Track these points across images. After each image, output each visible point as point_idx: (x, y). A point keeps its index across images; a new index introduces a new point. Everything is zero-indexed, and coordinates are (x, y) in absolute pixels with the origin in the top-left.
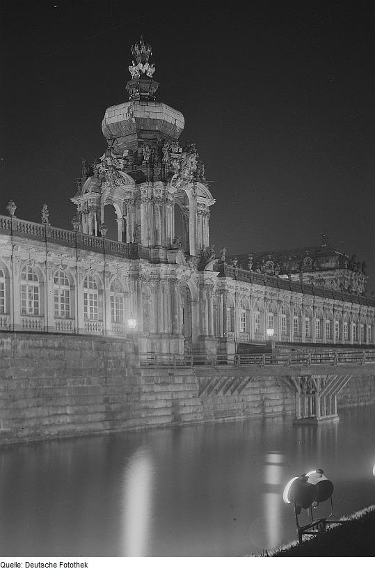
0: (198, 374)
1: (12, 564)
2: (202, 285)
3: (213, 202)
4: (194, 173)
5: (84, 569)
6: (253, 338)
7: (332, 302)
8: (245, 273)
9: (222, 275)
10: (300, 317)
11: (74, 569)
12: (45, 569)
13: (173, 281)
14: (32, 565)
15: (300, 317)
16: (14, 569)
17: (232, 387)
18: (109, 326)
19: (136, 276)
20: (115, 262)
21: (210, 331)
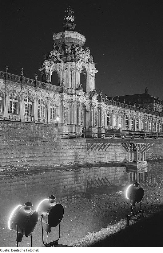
0: (87, 142)
1: (5, 250)
2: (91, 105)
3: (97, 72)
4: (89, 60)
5: (37, 252)
6: (113, 128)
7: (148, 115)
8: (110, 101)
9: (100, 101)
10: (134, 120)
11: (33, 252)
12: (20, 252)
13: (78, 103)
14: (14, 250)
15: (134, 120)
16: (6, 252)
17: (102, 148)
18: (49, 120)
19: (62, 100)
20: (53, 94)
21: (94, 124)
